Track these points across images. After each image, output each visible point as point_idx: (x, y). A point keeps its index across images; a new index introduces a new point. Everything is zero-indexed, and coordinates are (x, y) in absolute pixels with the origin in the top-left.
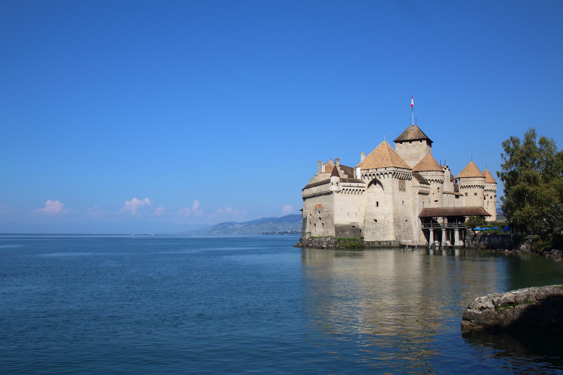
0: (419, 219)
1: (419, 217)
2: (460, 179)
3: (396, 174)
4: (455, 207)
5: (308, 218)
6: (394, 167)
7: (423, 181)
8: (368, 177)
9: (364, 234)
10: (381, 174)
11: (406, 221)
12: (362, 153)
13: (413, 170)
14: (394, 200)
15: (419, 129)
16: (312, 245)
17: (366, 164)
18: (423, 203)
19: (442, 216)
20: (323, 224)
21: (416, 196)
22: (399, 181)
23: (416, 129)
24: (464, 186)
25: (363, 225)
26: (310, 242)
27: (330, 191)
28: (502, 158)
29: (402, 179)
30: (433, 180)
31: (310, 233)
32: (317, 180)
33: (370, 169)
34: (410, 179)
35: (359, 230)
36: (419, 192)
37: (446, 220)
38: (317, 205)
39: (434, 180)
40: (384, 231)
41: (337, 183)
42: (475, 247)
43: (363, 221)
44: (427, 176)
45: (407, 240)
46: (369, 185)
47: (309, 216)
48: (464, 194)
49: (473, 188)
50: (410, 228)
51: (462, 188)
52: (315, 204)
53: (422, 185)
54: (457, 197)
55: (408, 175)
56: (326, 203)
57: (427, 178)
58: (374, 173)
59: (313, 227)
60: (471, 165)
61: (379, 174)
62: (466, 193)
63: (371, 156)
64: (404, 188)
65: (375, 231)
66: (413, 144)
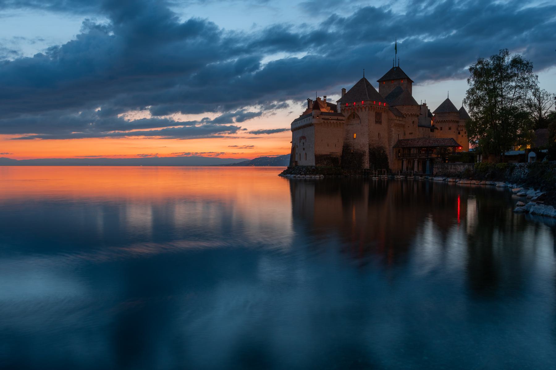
14: (370, 132)
21: (392, 129)
39: (410, 114)
48: (439, 128)
53: (398, 118)
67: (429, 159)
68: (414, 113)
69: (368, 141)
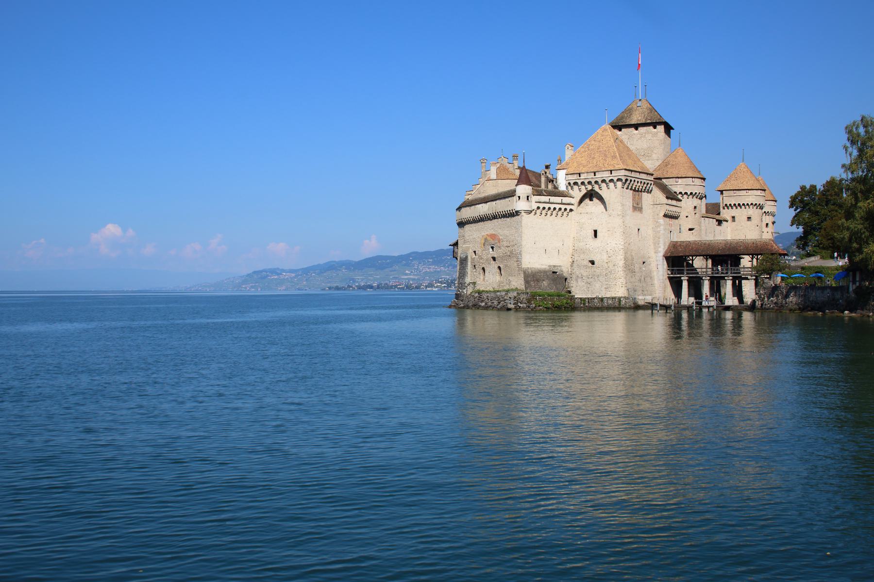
0: (663, 259)
1: (664, 256)
2: (724, 192)
3: (629, 182)
4: (725, 240)
5: (469, 258)
6: (626, 169)
7: (672, 196)
8: (579, 186)
9: (572, 285)
10: (604, 181)
11: (644, 263)
12: (568, 145)
13: (654, 176)
15: (651, 105)
16: (486, 304)
17: (575, 164)
18: (671, 232)
19: (703, 256)
20: (499, 268)
21: (659, 221)
22: (633, 193)
23: (645, 105)
24: (730, 205)
25: (570, 270)
26: (479, 299)
27: (514, 211)
28: (846, 153)
29: (638, 191)
30: (686, 193)
31: (474, 283)
32: (482, 191)
33: (583, 173)
34: (649, 192)
35: (564, 279)
36: (665, 214)
37: (710, 261)
38: (487, 235)
39: (689, 194)
40: (607, 280)
41: (528, 197)
42: (776, 307)
43: (570, 264)
44: (677, 187)
45: (645, 295)
46: (581, 201)
47: (471, 254)
48: (729, 218)
49: (745, 208)
50: (649, 276)
51: (726, 208)
52: (483, 234)
53: (670, 202)
54: (720, 222)
55: (648, 184)
56: (506, 232)
57: (677, 189)
58: (590, 180)
59: (479, 274)
60: (742, 169)
61: (600, 182)
62: (733, 217)
63: (583, 150)
64: (640, 206)
65: (591, 280)
66: (642, 131)
67: (731, 278)
68: (696, 192)
69: (622, 243)
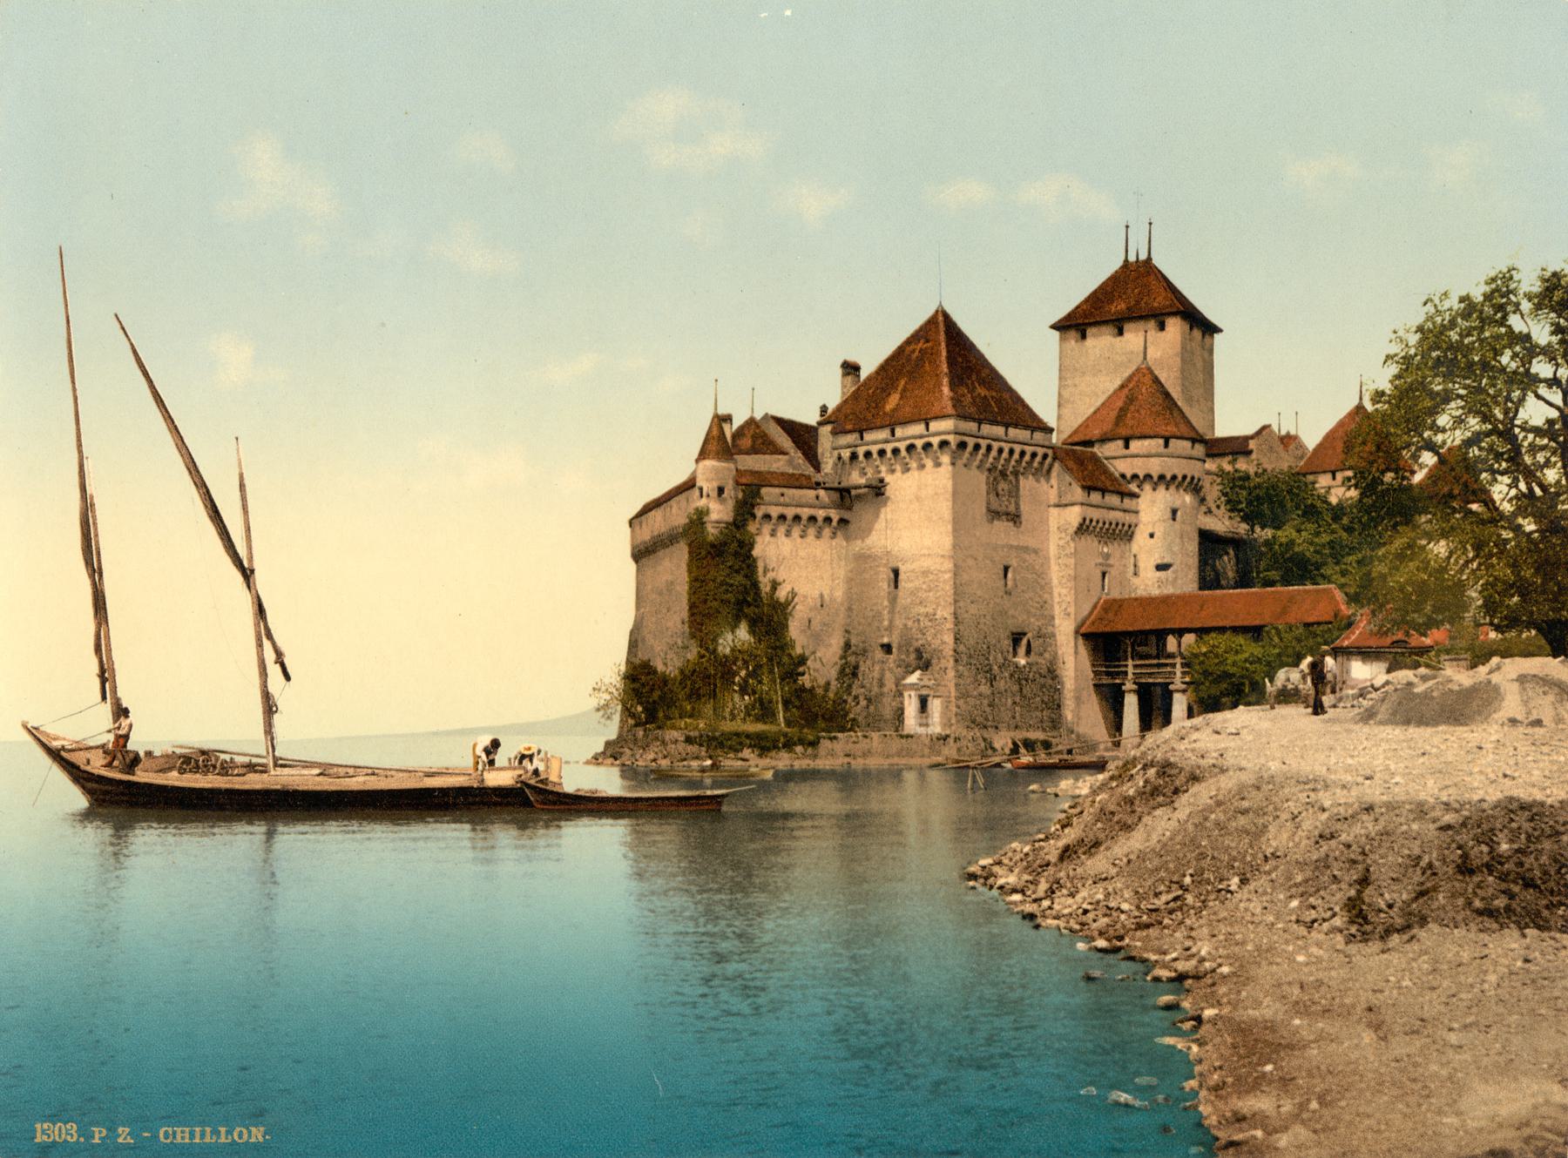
0: (1076, 638)
30: (1148, 477)
39: (1155, 479)
53: (1096, 497)
